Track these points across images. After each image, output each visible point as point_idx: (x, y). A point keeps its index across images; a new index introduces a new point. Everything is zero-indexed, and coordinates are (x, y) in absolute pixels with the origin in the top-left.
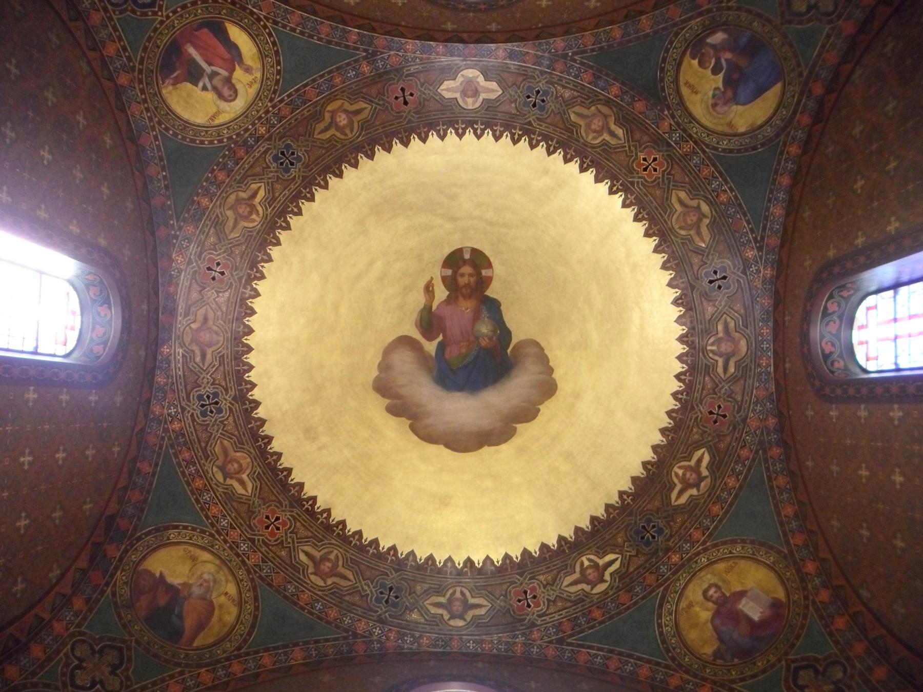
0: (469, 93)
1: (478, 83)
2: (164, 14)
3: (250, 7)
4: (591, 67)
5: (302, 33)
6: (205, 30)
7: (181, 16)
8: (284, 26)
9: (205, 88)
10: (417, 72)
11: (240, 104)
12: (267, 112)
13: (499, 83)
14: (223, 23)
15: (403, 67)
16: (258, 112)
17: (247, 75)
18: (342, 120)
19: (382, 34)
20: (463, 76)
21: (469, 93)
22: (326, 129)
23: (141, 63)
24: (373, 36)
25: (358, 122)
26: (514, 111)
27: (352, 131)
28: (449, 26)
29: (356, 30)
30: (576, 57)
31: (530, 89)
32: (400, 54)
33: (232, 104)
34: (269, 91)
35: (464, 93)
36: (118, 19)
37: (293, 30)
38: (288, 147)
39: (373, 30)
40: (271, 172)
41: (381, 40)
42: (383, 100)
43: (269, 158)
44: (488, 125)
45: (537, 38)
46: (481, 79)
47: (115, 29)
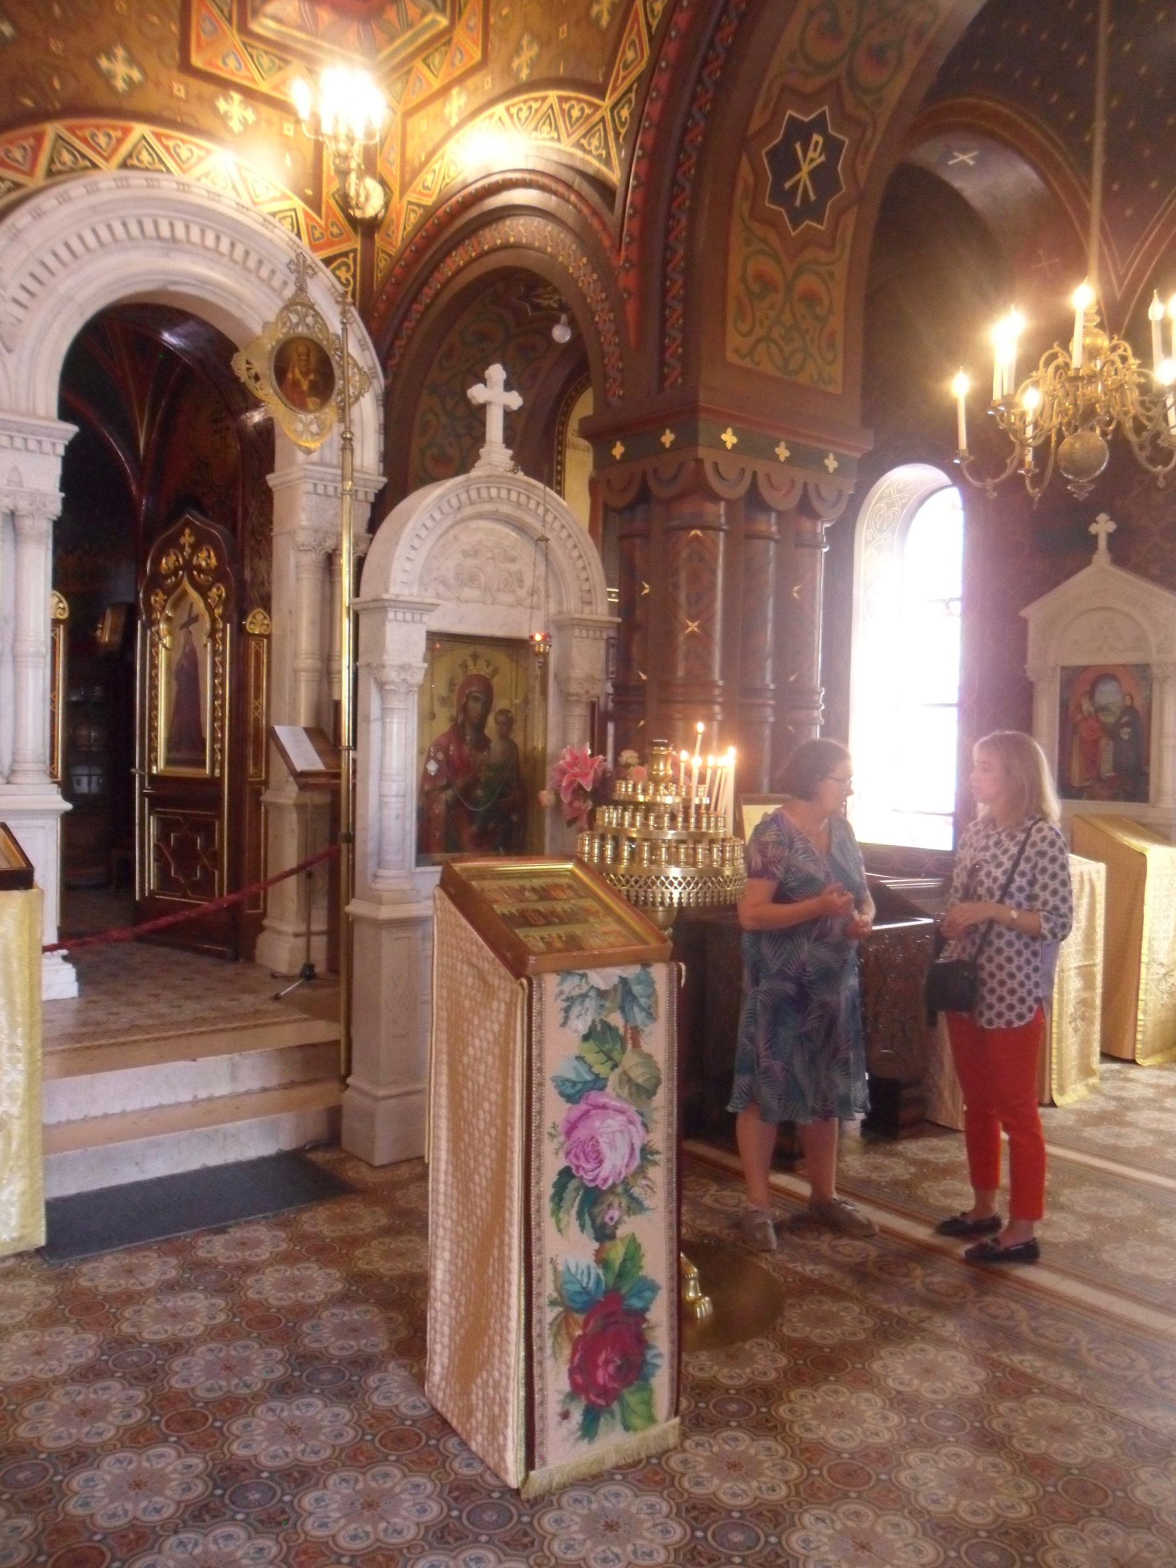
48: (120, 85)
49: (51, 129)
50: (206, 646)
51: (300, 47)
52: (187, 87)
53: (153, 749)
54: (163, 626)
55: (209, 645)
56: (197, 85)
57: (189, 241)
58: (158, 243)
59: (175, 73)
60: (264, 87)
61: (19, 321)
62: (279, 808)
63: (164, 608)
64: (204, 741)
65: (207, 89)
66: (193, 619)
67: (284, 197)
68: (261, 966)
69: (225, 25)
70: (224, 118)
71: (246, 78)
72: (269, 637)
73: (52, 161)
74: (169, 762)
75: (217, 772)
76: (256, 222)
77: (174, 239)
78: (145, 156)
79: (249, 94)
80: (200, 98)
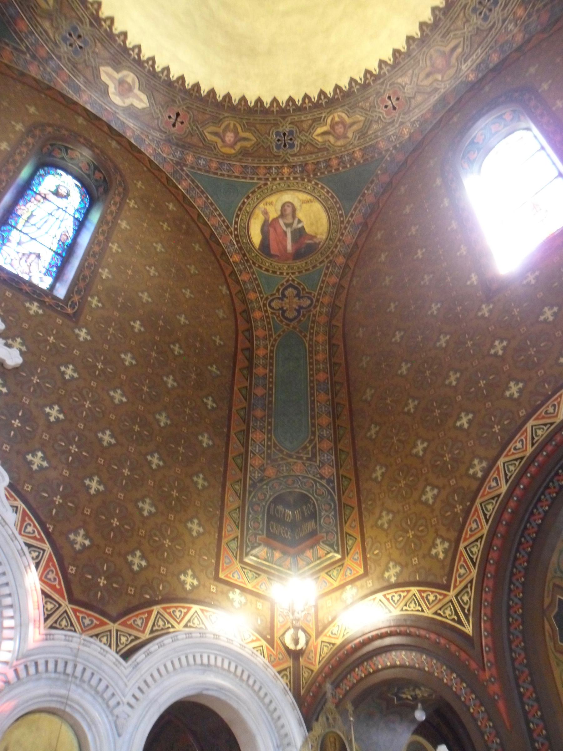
0: (126, 86)
1: (115, 89)
2: (288, 277)
3: (236, 246)
4: (16, 32)
5: (216, 210)
6: (272, 252)
7: (280, 269)
8: (224, 221)
9: (300, 221)
10: (157, 130)
11: (287, 197)
12: (274, 179)
13: (98, 76)
14: (260, 248)
15: (163, 140)
16: (279, 184)
17: (269, 211)
18: (230, 137)
19: (164, 172)
20: (124, 103)
21: (126, 86)
22: (245, 139)
23: (323, 261)
24: (171, 175)
25: (220, 127)
26: (99, 45)
27: (229, 124)
28: (114, 144)
29: (179, 187)
30: (24, 49)
31: (76, 52)
32: (160, 150)
33: (291, 201)
34: (262, 191)
35: (130, 89)
36: (316, 291)
37: (220, 215)
38: (278, 147)
39: (168, 179)
40: (302, 140)
41: (167, 169)
42: (192, 129)
43: (296, 150)
44: (125, 50)
45: (50, 88)
46: (112, 89)
47: (321, 288)
48: (188, 587)
49: (156, 609)
51: (264, 568)
52: (217, 587)
56: (222, 586)
57: (216, 665)
58: (200, 667)
59: (212, 581)
60: (249, 586)
61: (128, 716)
65: (226, 588)
67: (257, 640)
69: (234, 559)
70: (232, 601)
71: (241, 582)
73: (154, 625)
76: (249, 653)
77: (209, 665)
78: (196, 621)
79: (243, 590)
80: (222, 592)
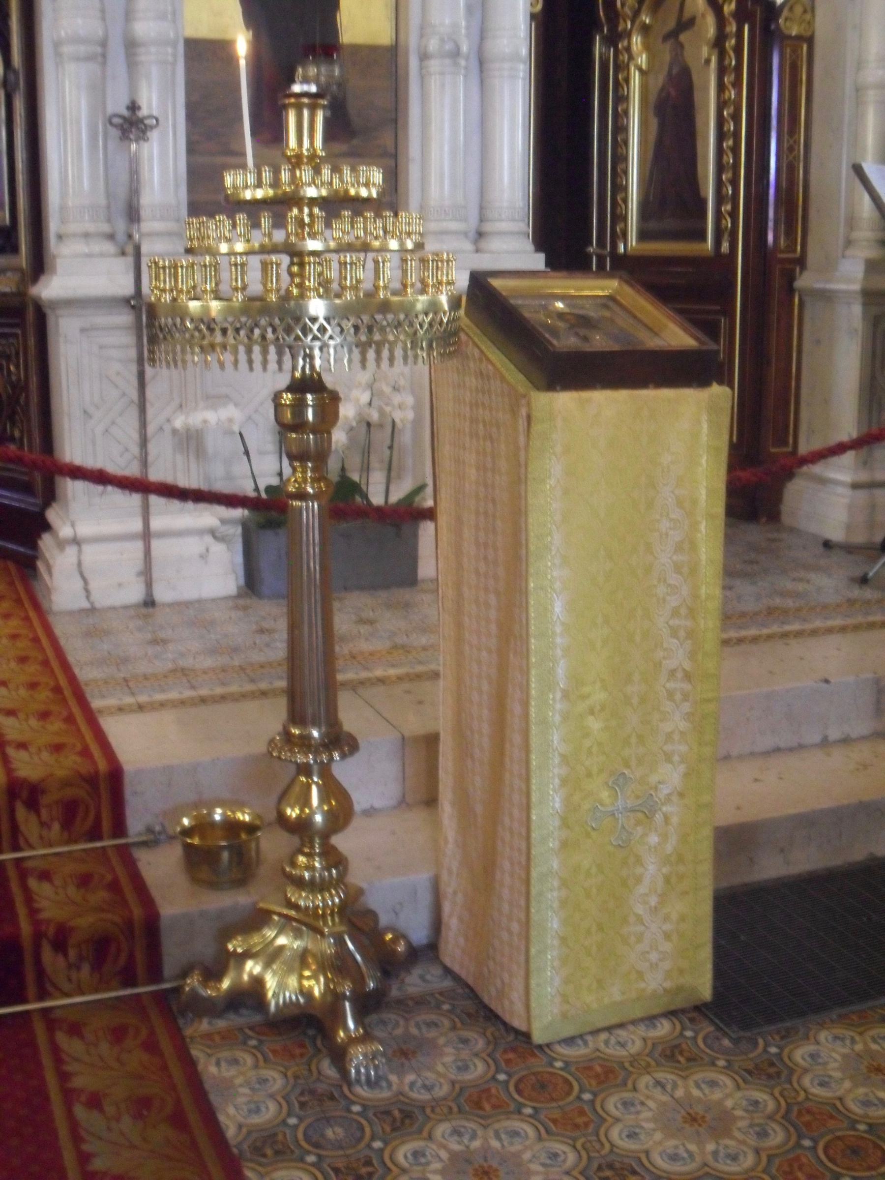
50: (708, 61)
53: (620, 218)
54: (637, 41)
55: (714, 60)
62: (826, 297)
63: (636, 13)
64: (703, 202)
66: (686, 24)
68: (792, 530)
72: (810, 41)
74: (643, 235)
75: (725, 247)
